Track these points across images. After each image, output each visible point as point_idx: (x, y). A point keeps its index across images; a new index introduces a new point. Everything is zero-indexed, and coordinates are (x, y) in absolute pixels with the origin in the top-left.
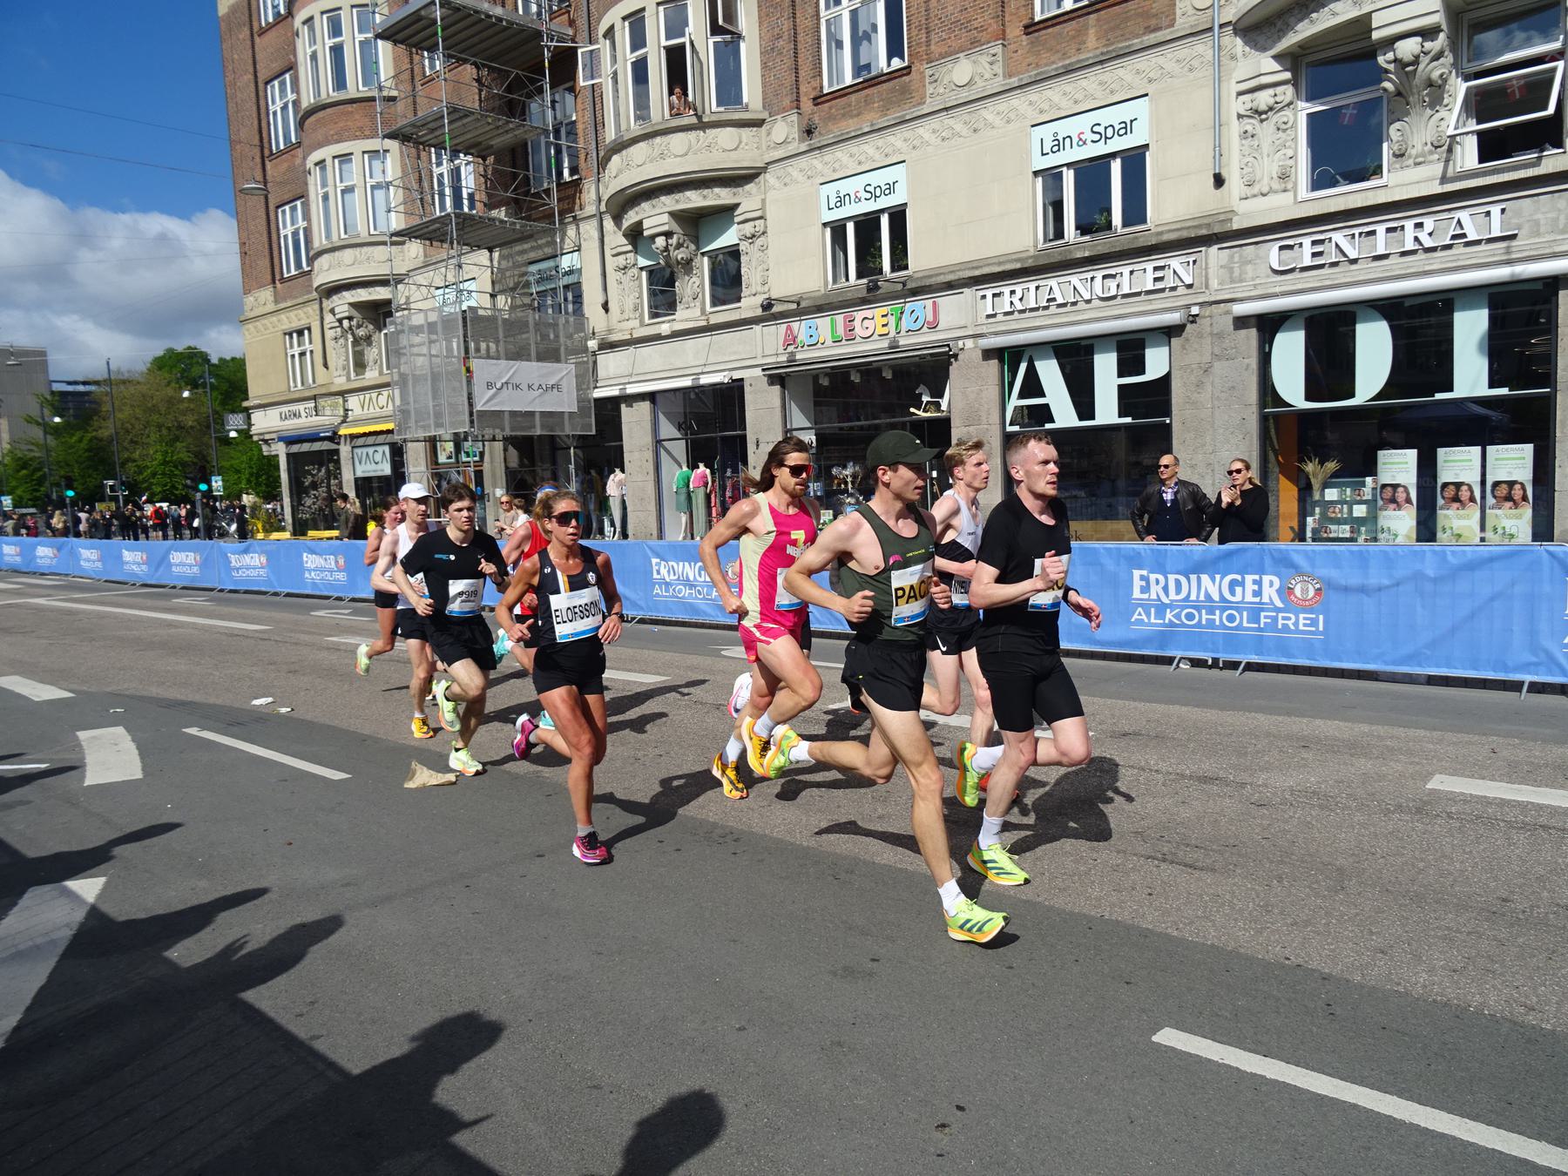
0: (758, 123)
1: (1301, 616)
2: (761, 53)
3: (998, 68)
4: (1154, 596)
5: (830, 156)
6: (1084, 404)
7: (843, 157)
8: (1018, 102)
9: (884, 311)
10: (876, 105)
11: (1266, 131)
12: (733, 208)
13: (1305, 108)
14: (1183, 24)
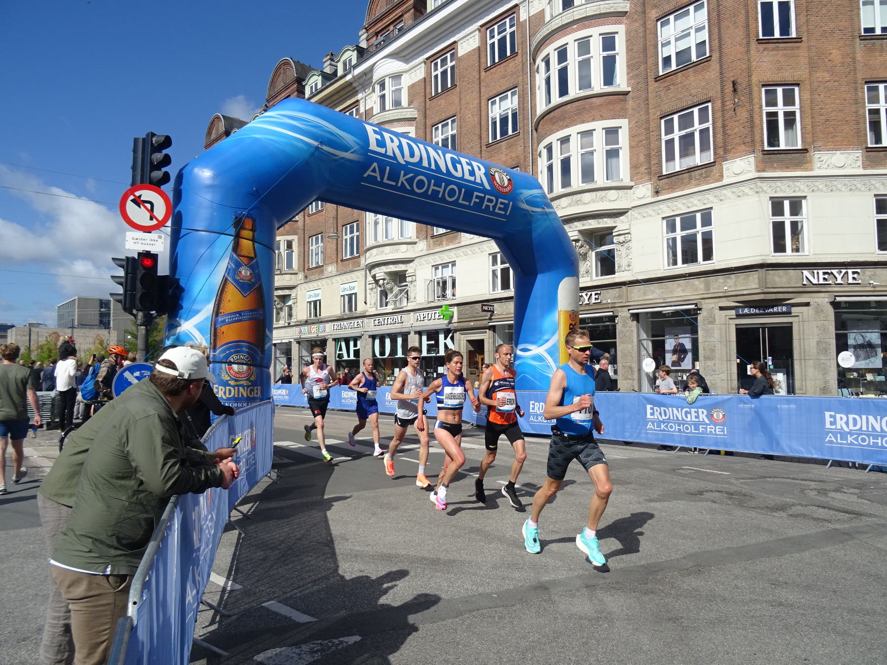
0: (296, 274)
1: (717, 427)
4: (656, 417)
5: (310, 284)
8: (338, 278)
9: (316, 326)
11: (372, 293)
12: (291, 295)
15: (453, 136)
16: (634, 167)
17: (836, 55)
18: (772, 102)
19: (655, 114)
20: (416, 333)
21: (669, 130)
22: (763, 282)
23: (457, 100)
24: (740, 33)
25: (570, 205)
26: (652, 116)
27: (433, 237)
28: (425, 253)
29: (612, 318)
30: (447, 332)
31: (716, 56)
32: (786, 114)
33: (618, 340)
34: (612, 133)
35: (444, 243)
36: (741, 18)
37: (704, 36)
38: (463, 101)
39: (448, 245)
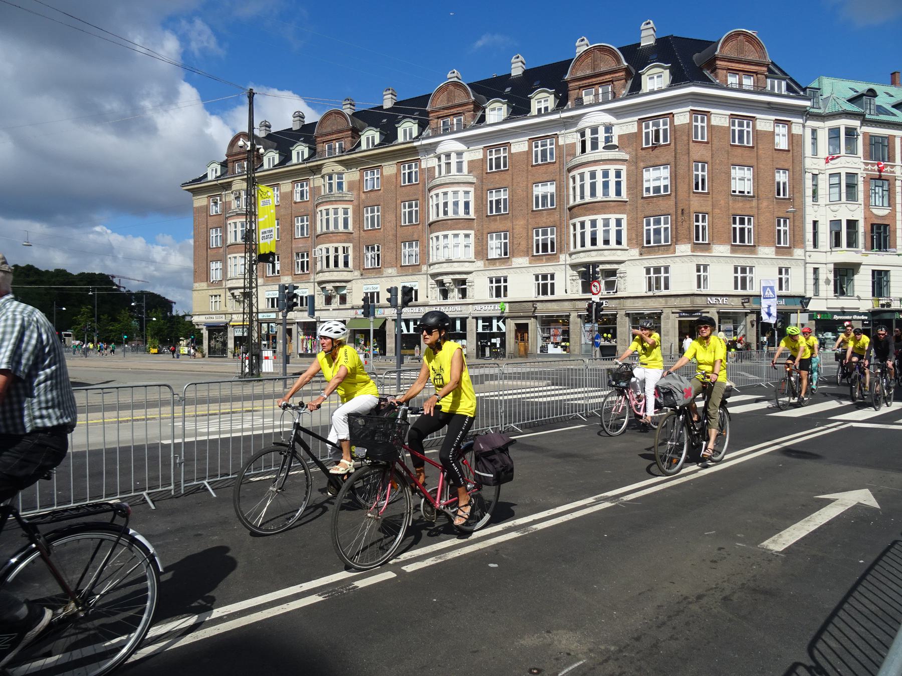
6: (408, 330)
8: (398, 278)
14: (423, 272)
15: (505, 200)
16: (629, 240)
17: (722, 202)
18: (697, 221)
19: (640, 215)
20: (473, 318)
21: (648, 224)
22: (692, 302)
23: (509, 179)
24: (686, 187)
25: (596, 256)
26: (639, 216)
27: (488, 260)
29: (615, 315)
30: (499, 318)
31: (673, 194)
32: (703, 226)
33: (618, 326)
34: (619, 222)
35: (497, 264)
36: (687, 180)
37: (667, 182)
38: (515, 181)
39: (500, 266)
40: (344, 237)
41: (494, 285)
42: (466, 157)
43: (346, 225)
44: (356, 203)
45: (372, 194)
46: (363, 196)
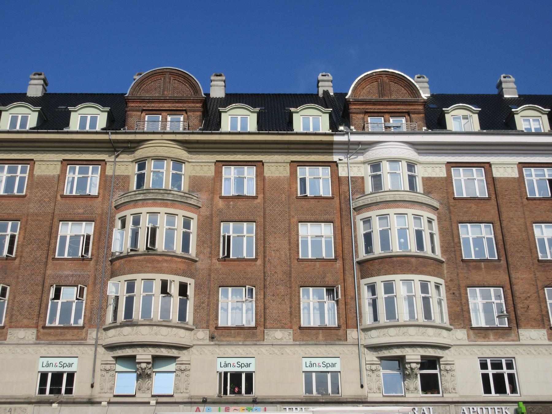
0: (191, 330)
2: (194, 306)
3: (291, 337)
7: (229, 350)
10: (242, 336)
11: (374, 376)
13: (382, 372)
28: (467, 342)
35: (491, 337)
39: (497, 340)
40: (183, 266)
41: (490, 372)
42: (421, 172)
43: (186, 247)
44: (205, 211)
45: (240, 203)
46: (221, 204)
